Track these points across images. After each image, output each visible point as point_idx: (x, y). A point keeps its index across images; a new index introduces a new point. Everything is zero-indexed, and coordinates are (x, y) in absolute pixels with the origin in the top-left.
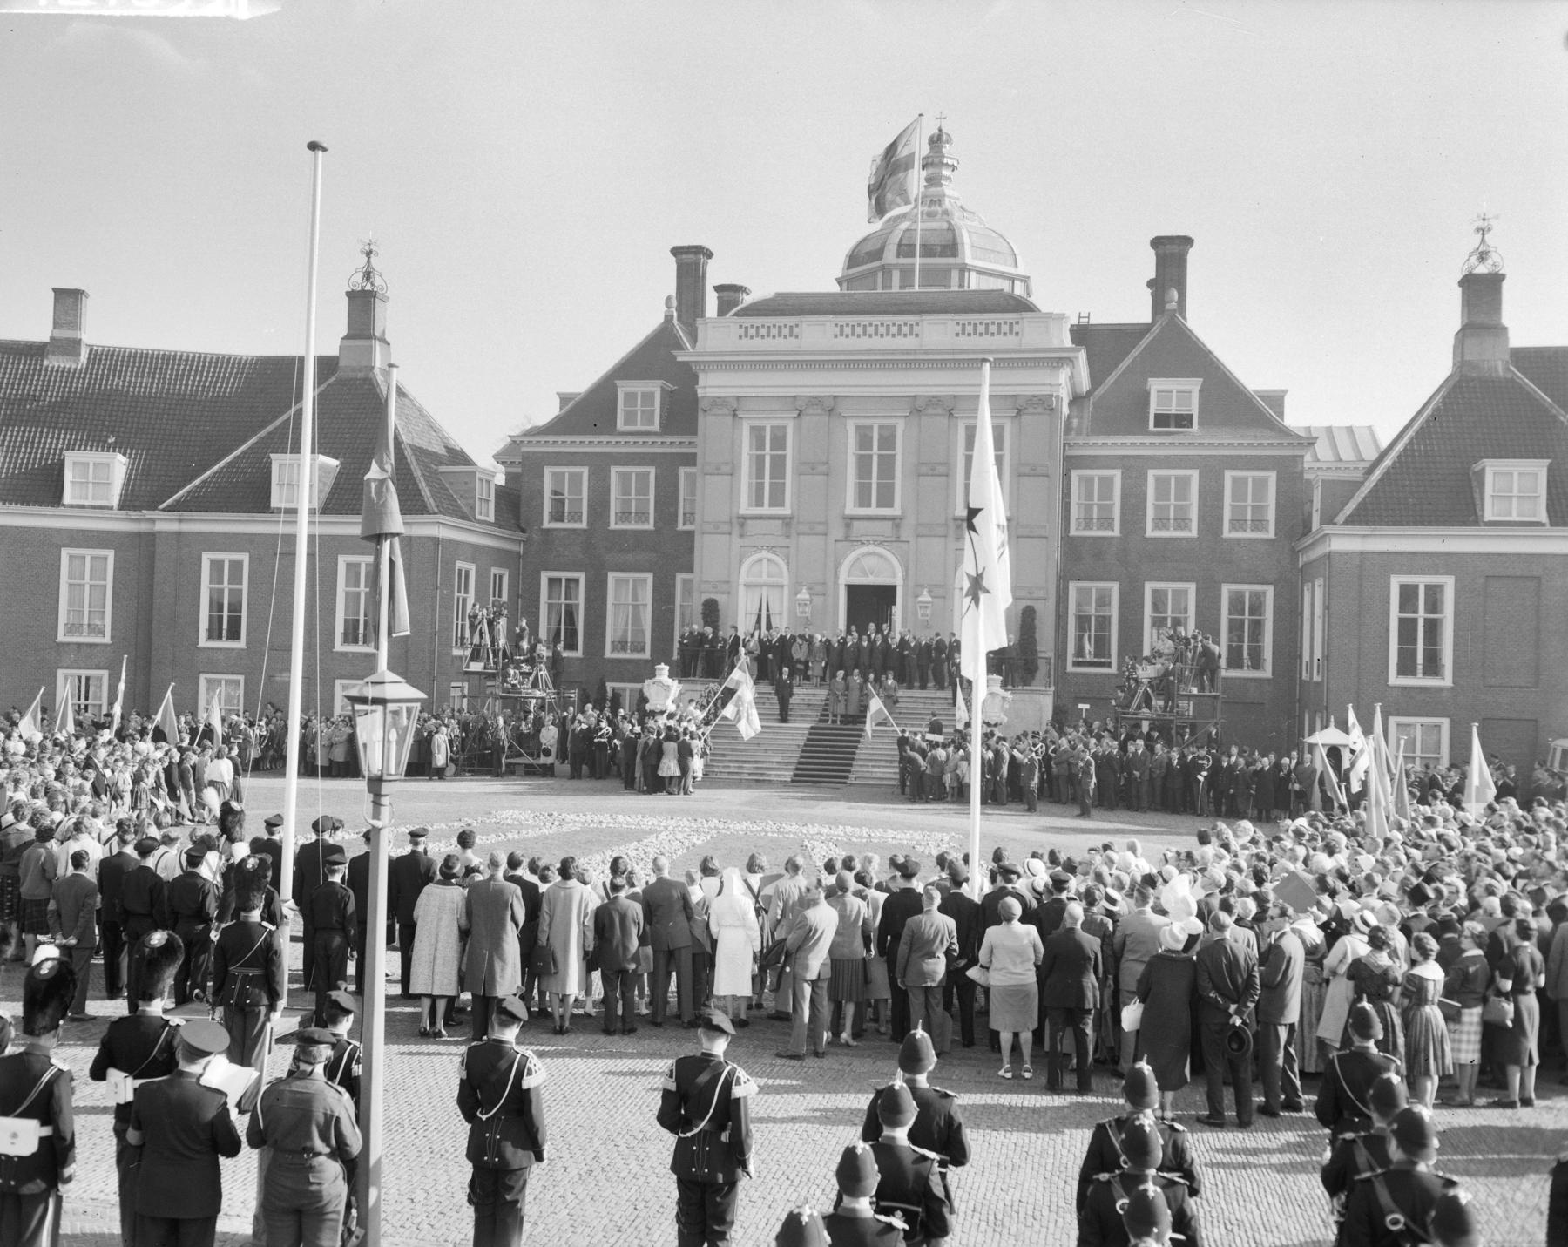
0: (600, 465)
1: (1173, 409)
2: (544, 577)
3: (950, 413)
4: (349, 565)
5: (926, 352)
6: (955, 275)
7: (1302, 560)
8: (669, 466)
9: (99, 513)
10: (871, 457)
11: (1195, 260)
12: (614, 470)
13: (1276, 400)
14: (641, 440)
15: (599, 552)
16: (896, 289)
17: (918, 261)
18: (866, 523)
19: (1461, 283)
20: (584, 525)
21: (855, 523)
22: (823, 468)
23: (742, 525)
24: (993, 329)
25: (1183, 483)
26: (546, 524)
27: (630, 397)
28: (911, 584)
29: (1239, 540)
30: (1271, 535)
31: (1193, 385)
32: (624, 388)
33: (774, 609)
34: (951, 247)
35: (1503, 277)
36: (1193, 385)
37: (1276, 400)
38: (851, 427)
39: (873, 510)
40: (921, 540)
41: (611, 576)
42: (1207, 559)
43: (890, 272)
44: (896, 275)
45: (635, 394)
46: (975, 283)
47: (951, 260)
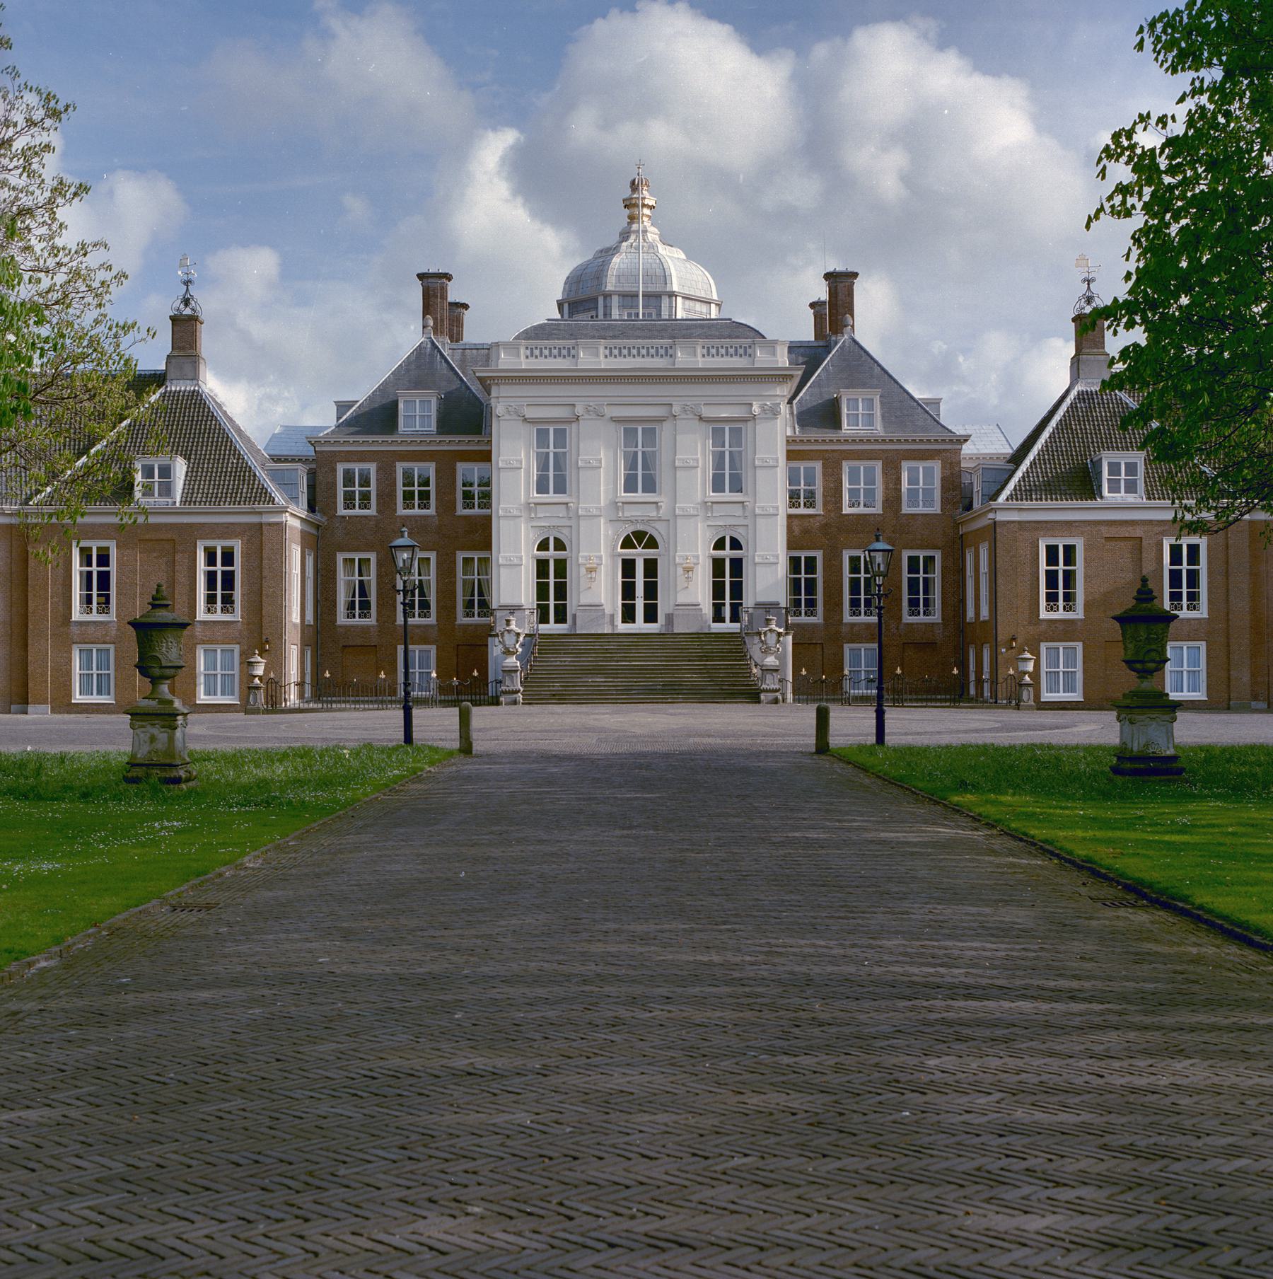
0: (386, 462)
2: (340, 557)
8: (446, 462)
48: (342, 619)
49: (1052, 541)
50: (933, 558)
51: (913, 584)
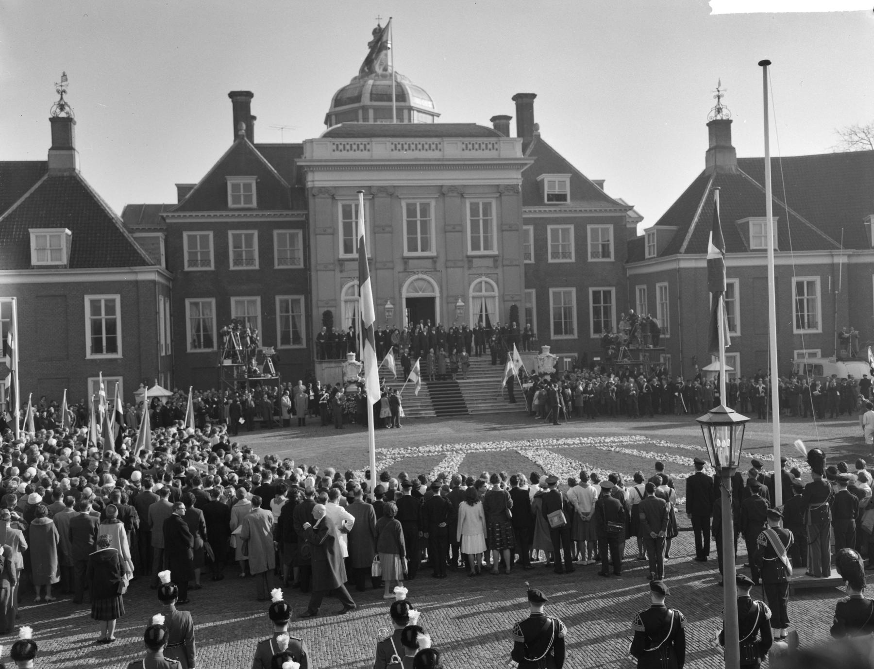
1: (557, 191)
2: (187, 302)
3: (462, 196)
4: (92, 302)
5: (449, 160)
6: (406, 112)
7: (630, 272)
8: (266, 230)
9: (53, 271)
10: (416, 221)
11: (538, 106)
12: (230, 233)
13: (601, 183)
14: (242, 213)
15: (221, 285)
16: (371, 122)
17: (394, 104)
18: (415, 261)
19: (708, 125)
20: (212, 268)
21: (410, 261)
22: (388, 229)
23: (341, 265)
24: (483, 146)
25: (566, 232)
26: (186, 269)
27: (236, 187)
28: (445, 296)
29: (596, 263)
30: (612, 259)
31: (566, 178)
32: (231, 181)
34: (402, 96)
35: (731, 121)
36: (566, 178)
37: (601, 183)
38: (404, 204)
39: (419, 253)
40: (450, 270)
41: (233, 300)
42: (578, 274)
43: (367, 110)
44: (371, 113)
45: (239, 185)
46: (418, 119)
47: (402, 104)
48: (189, 350)
49: (800, 279)
50: (609, 292)
51: (597, 311)
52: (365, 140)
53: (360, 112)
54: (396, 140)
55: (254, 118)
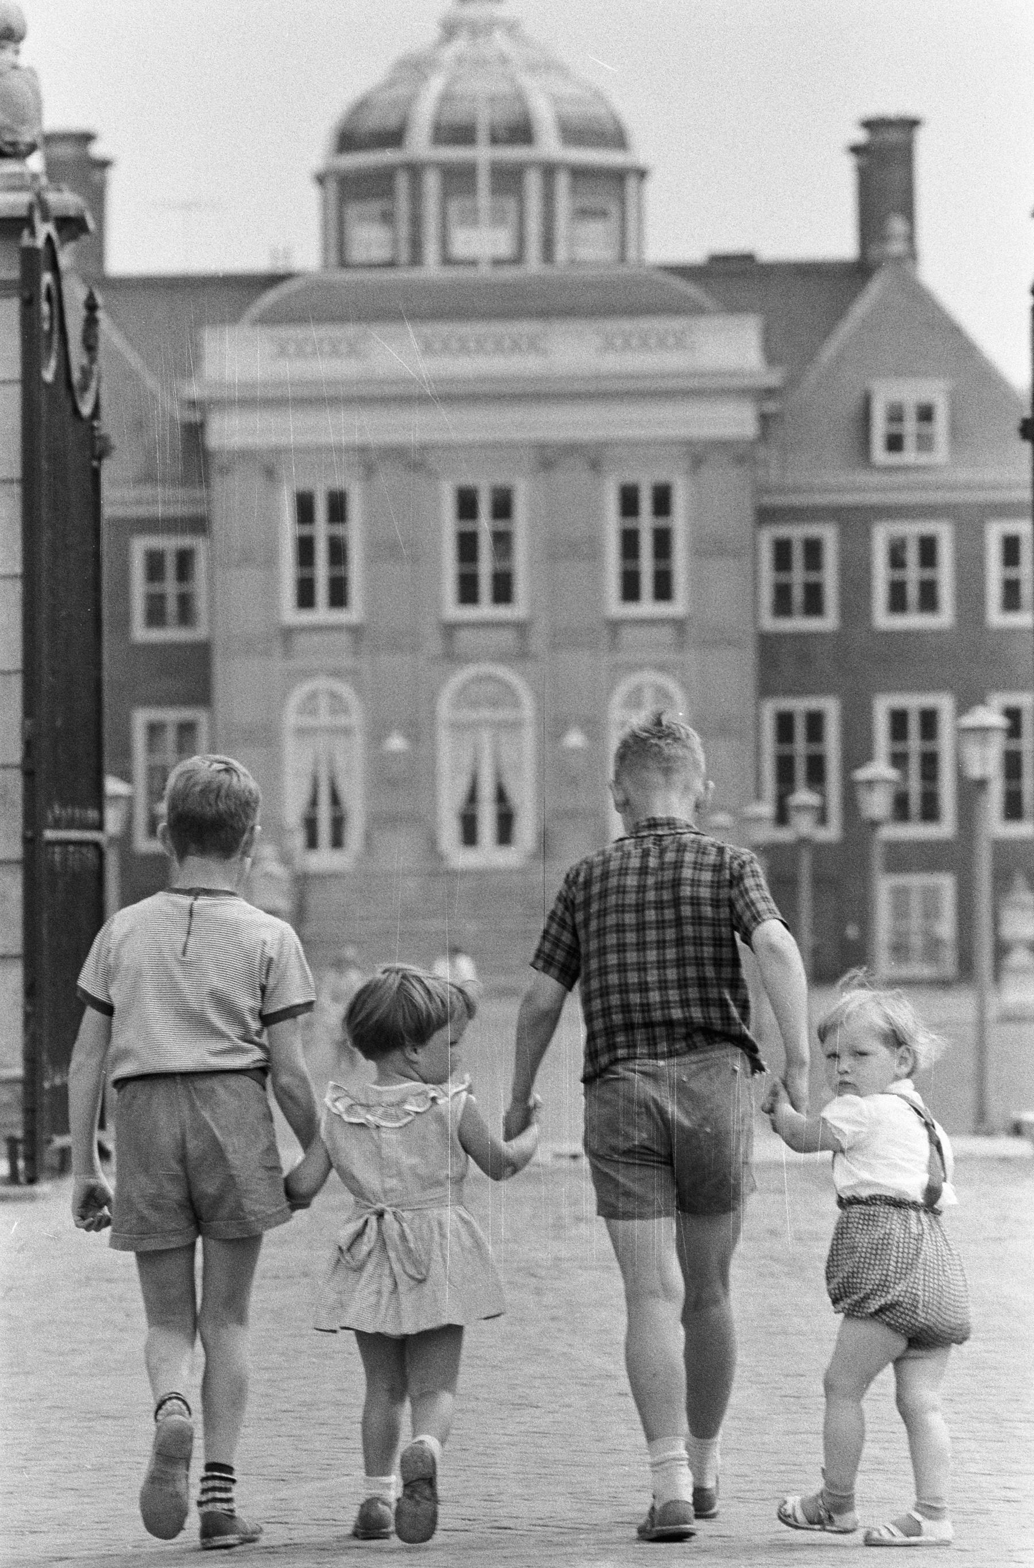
33: (341, 762)
52: (351, 330)
53: (402, 183)
54: (428, 329)
55: (104, 164)
